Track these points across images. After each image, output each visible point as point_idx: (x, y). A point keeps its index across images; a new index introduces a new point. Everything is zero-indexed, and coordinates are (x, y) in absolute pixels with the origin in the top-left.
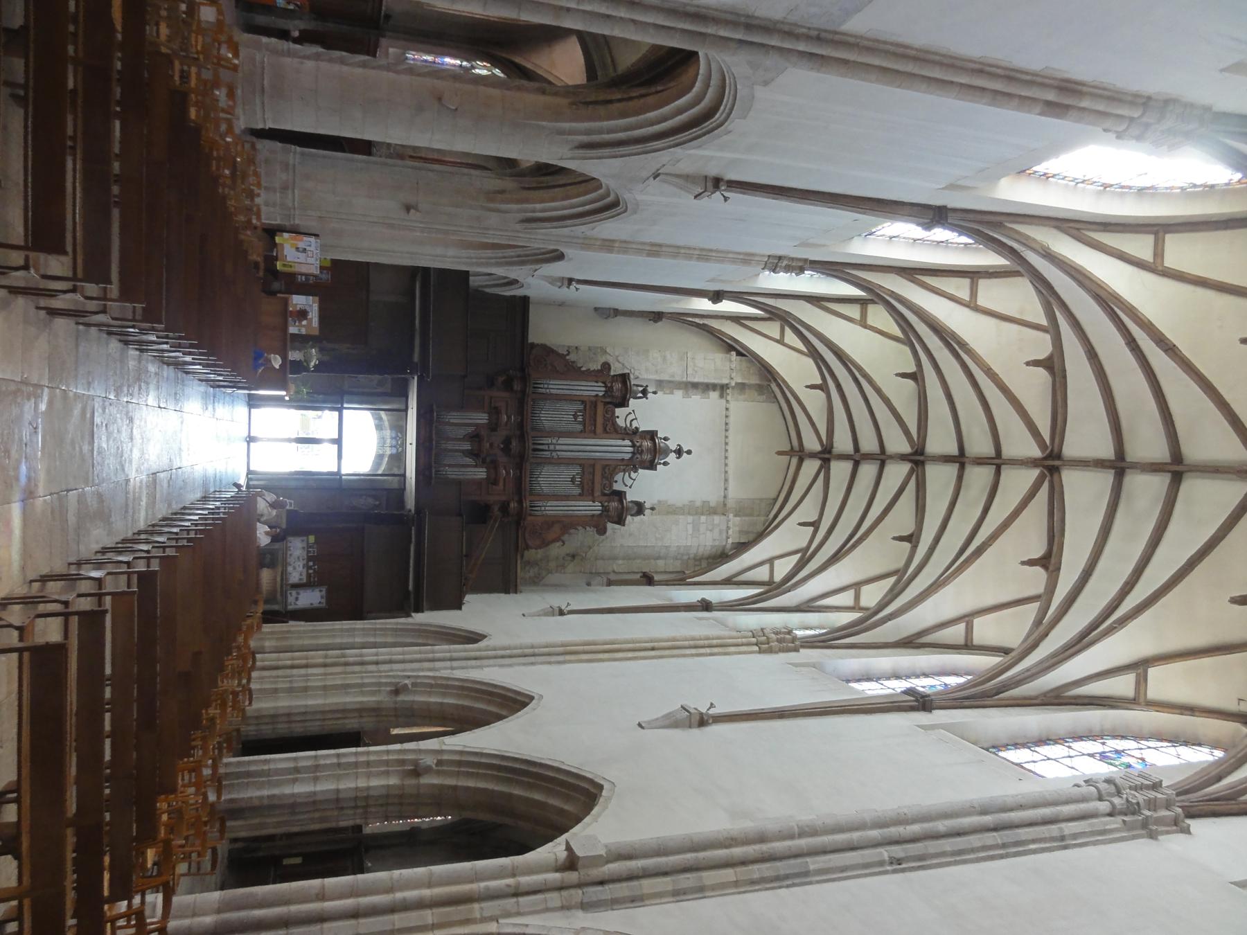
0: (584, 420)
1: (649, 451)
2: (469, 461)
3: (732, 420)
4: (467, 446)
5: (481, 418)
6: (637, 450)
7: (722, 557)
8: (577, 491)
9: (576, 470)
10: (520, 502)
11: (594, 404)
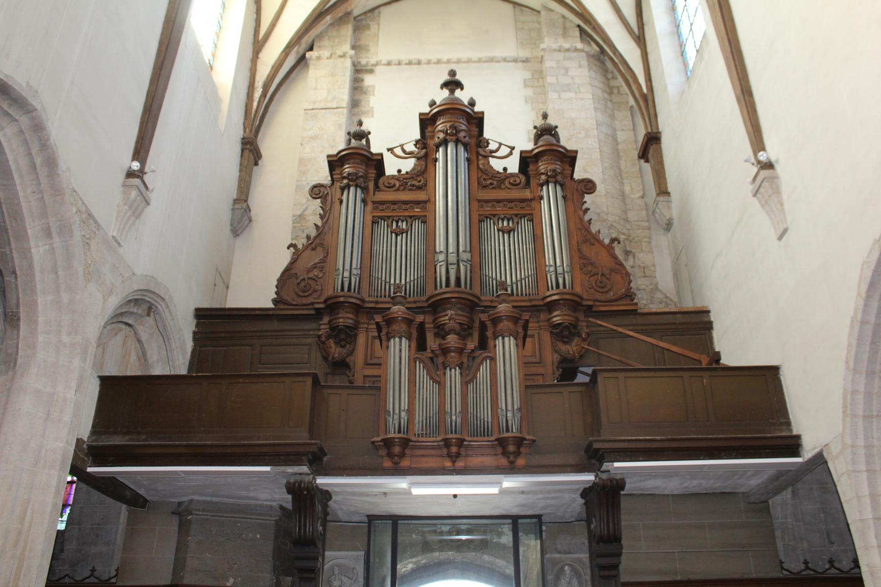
0: (405, 219)
1: (454, 124)
2: (484, 371)
3: (405, 57)
4: (454, 376)
5: (399, 350)
6: (453, 137)
7: (604, 57)
8: (525, 225)
9: (491, 229)
10: (551, 306)
11: (377, 204)
